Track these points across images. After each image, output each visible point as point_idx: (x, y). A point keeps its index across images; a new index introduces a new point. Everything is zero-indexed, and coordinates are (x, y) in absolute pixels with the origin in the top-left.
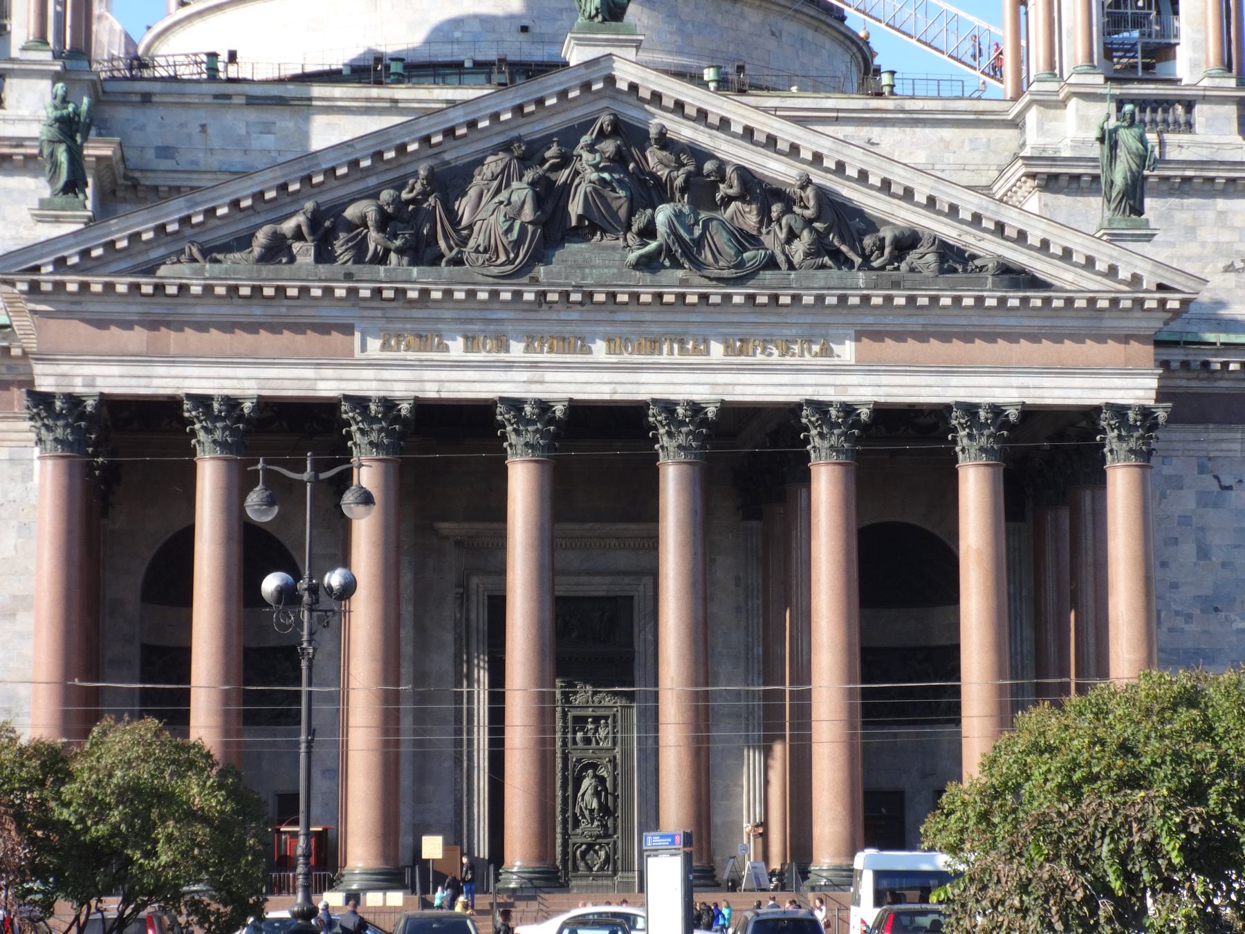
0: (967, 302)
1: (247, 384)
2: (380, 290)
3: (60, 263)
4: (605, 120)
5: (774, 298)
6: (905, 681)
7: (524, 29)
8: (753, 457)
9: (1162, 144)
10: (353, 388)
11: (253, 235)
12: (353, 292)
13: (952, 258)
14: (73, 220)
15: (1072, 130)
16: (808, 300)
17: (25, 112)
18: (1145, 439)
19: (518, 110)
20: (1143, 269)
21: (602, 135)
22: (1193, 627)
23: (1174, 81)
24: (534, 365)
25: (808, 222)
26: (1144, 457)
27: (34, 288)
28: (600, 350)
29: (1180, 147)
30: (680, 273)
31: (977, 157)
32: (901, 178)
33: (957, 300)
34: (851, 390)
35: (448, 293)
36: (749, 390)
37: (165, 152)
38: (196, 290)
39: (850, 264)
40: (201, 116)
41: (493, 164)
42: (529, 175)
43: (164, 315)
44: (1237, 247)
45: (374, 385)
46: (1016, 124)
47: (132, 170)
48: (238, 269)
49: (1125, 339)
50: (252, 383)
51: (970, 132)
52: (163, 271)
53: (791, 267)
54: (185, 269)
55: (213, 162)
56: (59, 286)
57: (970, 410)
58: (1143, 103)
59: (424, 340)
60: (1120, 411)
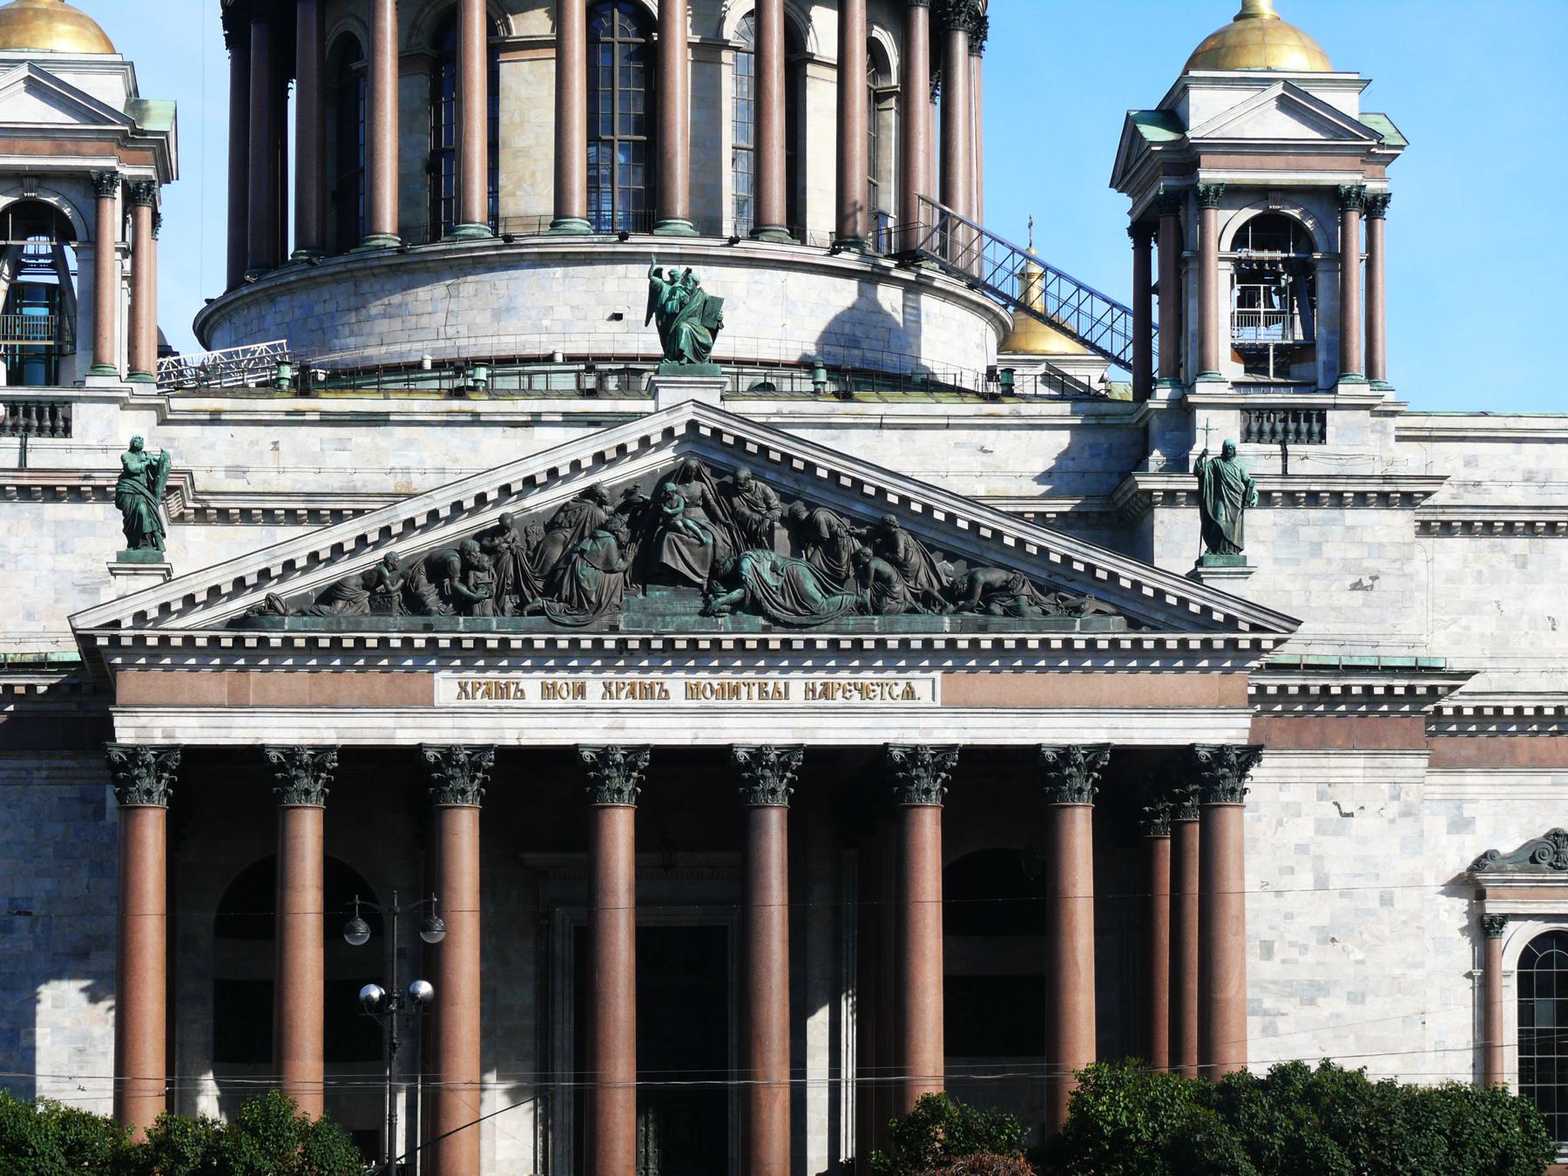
1: (326, 733)
2: (459, 640)
7: (618, 317)
9: (1285, 456)
12: (432, 642)
17: (93, 442)
24: (615, 711)
27: (114, 640)
30: (761, 621)
34: (936, 733)
36: (833, 733)
37: (236, 471)
44: (1366, 564)
45: (456, 733)
47: (202, 493)
50: (332, 733)
56: (140, 640)
58: (1261, 411)
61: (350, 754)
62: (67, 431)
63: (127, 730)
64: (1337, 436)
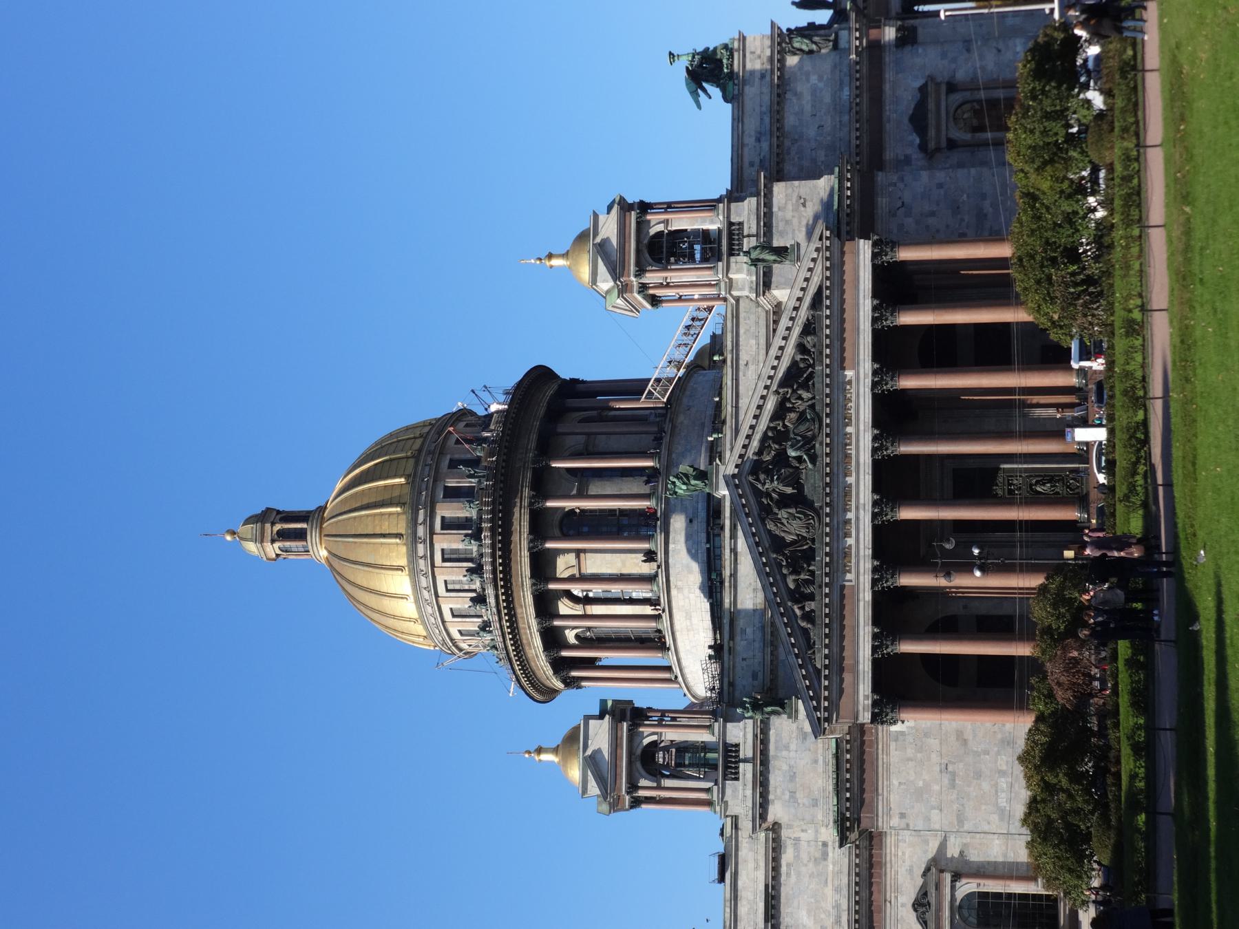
0: (828, 322)
3: (816, 709)
4: (750, 478)
5: (827, 405)
6: (991, 347)
7: (691, 521)
8: (894, 414)
9: (749, 236)
10: (868, 585)
11: (802, 628)
13: (808, 329)
14: (796, 704)
15: (742, 274)
16: (828, 391)
18: (887, 243)
19: (747, 515)
20: (813, 246)
21: (758, 479)
22: (966, 218)
23: (720, 231)
24: (857, 508)
25: (794, 391)
26: (895, 245)
27: (826, 720)
28: (851, 480)
29: (751, 226)
31: (753, 317)
32: (774, 351)
33: (827, 327)
35: (827, 544)
38: (827, 651)
39: (812, 373)
40: (738, 660)
41: (771, 526)
42: (776, 510)
43: (838, 665)
46: (737, 300)
48: (818, 634)
49: (843, 253)
51: (741, 320)
52: (819, 666)
53: (813, 398)
54: (818, 656)
55: (759, 655)
57: (874, 320)
58: (730, 245)
59: (847, 555)
60: (874, 256)
61: (876, 621)
62: (737, 745)
63: (865, 717)
64: (740, 216)
